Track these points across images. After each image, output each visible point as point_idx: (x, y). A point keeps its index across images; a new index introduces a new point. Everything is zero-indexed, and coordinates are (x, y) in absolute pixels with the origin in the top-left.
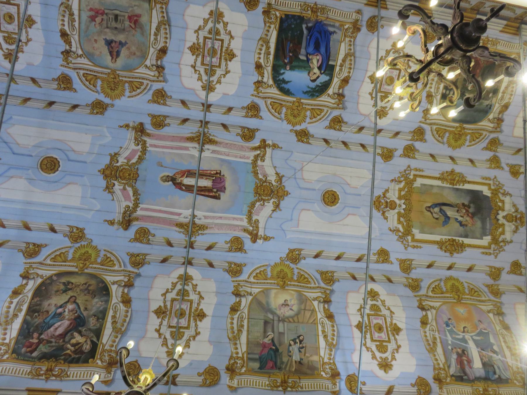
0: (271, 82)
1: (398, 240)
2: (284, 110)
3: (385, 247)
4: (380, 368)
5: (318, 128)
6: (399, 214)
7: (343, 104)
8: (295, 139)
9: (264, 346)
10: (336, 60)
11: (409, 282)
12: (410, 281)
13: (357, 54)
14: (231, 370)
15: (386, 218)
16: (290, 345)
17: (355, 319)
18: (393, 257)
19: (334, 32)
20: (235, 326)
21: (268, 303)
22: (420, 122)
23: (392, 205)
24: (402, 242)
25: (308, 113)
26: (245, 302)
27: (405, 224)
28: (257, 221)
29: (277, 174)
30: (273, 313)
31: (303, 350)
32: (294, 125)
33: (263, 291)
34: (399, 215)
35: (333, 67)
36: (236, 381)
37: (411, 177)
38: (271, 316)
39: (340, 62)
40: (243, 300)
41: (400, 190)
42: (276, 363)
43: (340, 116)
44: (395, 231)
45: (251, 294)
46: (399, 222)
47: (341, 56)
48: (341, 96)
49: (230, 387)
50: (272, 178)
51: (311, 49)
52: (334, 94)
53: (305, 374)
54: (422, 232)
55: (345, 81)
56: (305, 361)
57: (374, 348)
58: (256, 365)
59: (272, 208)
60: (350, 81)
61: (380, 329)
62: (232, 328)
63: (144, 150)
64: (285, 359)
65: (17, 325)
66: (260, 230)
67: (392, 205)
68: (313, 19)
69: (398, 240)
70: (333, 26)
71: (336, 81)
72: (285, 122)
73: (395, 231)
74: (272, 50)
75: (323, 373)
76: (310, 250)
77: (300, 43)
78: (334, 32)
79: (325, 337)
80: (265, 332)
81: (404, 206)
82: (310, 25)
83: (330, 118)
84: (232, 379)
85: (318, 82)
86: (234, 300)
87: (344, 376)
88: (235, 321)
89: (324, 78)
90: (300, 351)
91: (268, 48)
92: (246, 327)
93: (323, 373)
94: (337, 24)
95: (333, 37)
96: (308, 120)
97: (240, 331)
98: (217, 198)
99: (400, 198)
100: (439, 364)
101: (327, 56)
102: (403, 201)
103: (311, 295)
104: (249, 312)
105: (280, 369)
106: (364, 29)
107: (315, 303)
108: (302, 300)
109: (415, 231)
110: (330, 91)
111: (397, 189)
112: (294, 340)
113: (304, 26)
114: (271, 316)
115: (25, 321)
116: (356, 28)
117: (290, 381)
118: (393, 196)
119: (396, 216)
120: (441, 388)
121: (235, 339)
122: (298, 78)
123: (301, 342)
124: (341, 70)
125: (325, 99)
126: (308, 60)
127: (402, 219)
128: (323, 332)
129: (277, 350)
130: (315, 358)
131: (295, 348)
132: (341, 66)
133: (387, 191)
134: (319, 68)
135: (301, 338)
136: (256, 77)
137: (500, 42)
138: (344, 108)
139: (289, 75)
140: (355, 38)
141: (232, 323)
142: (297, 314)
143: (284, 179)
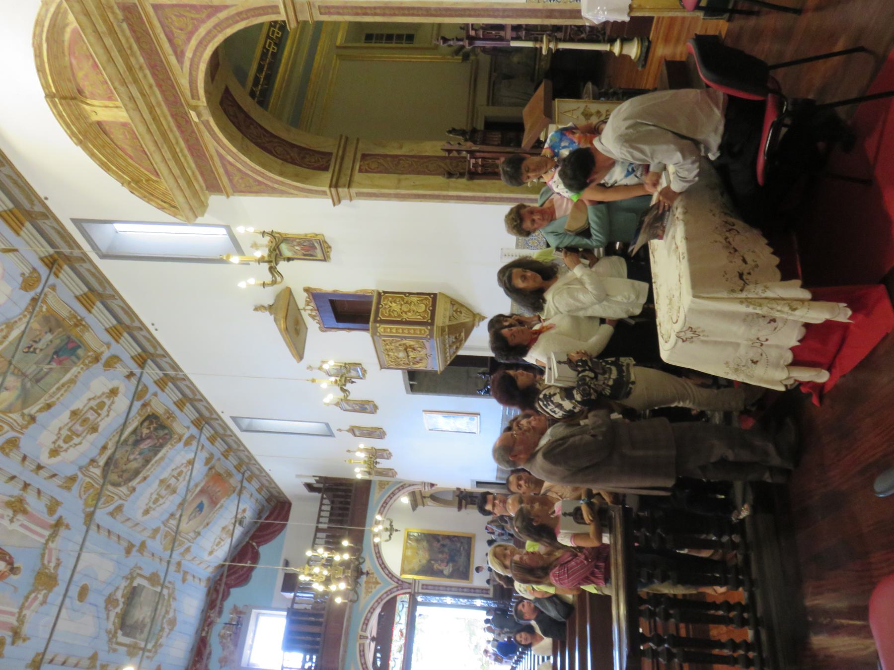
9: (60, 363)
14: (97, 359)
16: (41, 350)
20: (62, 392)
21: (17, 398)
26: (33, 410)
30: (23, 386)
31: (37, 339)
33: (10, 412)
36: (102, 349)
38: (29, 385)
42: (67, 344)
45: (23, 415)
49: (109, 348)
53: (56, 319)
56: (46, 329)
58: (80, 352)
62: (65, 391)
63: (21, 609)
64: (58, 341)
65: (160, 455)
75: (44, 309)
80: (47, 374)
84: (102, 353)
86: (40, 417)
88: (59, 395)
90: (40, 340)
92: (57, 386)
93: (44, 309)
97: (63, 386)
104: (40, 398)
105: (69, 337)
112: (34, 352)
114: (29, 385)
115: (156, 454)
117: (72, 323)
121: (72, 381)
123: (29, 348)
129: (56, 353)
135: (27, 350)
141: (62, 395)
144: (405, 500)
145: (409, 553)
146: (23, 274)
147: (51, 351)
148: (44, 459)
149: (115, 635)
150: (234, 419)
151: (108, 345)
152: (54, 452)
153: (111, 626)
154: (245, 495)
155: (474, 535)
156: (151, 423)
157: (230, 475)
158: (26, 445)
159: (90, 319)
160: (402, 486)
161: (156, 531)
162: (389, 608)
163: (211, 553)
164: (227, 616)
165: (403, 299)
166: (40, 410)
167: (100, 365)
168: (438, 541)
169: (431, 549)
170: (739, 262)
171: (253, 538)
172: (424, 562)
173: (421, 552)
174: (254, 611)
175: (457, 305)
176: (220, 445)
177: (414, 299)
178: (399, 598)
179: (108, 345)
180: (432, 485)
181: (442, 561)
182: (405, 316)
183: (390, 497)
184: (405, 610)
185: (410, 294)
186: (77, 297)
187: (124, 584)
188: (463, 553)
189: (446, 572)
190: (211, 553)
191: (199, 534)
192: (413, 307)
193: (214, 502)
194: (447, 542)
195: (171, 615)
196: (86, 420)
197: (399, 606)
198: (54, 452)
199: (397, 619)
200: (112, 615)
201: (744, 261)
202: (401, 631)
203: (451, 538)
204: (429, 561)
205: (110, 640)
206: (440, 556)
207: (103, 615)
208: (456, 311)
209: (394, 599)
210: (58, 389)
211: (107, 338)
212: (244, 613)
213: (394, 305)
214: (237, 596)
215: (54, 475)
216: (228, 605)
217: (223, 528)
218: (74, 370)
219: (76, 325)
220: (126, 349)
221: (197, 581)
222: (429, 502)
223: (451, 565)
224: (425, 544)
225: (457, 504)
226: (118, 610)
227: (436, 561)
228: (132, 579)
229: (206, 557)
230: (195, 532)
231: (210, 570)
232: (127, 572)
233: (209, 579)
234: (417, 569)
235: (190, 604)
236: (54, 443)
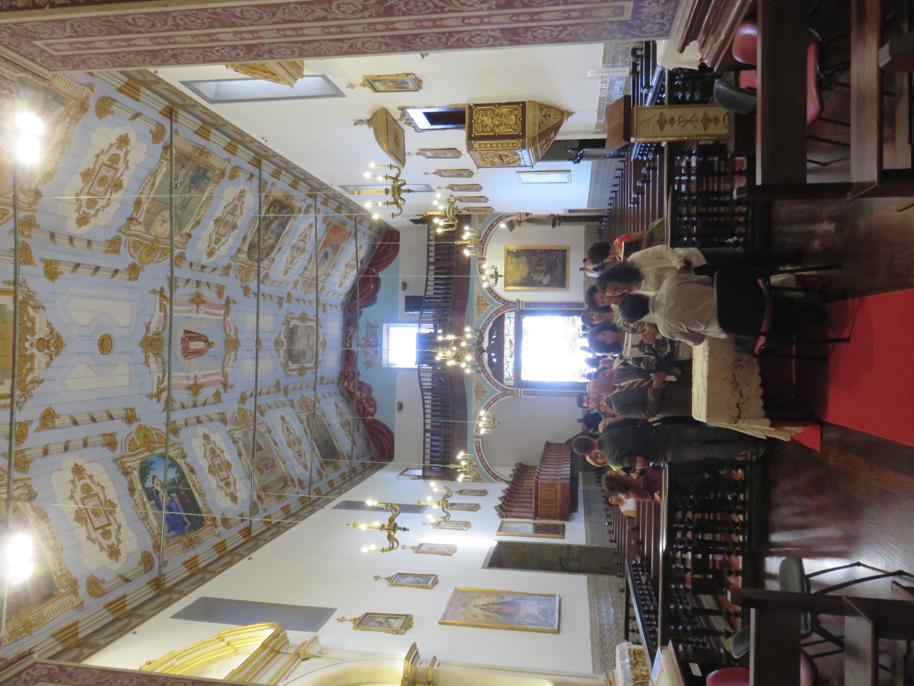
0: (178, 460)
1: (34, 293)
2: (156, 438)
3: (49, 282)
4: (129, 141)
5: (122, 430)
6: (33, 333)
7: (119, 465)
8: (136, 411)
9: (197, 188)
10: (152, 506)
11: (29, 231)
12: (26, 233)
13: (140, 522)
14: (223, 174)
15: (49, 324)
18: (40, 268)
19: (168, 532)
23: (42, 344)
24: (29, 291)
25: (138, 443)
26: (187, 229)
27: (25, 318)
28: (161, 310)
29: (149, 365)
32: (140, 426)
34: (32, 331)
35: (150, 499)
38: (179, 213)
39: (148, 506)
40: (188, 231)
41: (31, 369)
43: (113, 451)
44: (38, 307)
45: (181, 235)
46: (32, 320)
48: (126, 473)
49: (229, 162)
50: (152, 359)
52: (132, 472)
55: (132, 490)
56: (180, 167)
58: (209, 174)
59: (151, 325)
60: (128, 492)
61: (102, 180)
63: (223, 368)
64: (191, 173)
65: (287, 228)
66: (158, 301)
67: (42, 344)
68: (187, 534)
69: (34, 293)
70: (173, 537)
71: (138, 486)
72: (148, 427)
73: (38, 307)
74: (194, 491)
76: (122, 278)
78: (168, 532)
79: (153, 185)
81: (27, 345)
82: (186, 528)
83: (119, 445)
85: (150, 477)
86: (194, 233)
87: (162, 143)
89: (149, 484)
91: (197, 490)
94: (171, 541)
96: (134, 435)
98: (186, 332)
99: (32, 356)
100: (69, 123)
102: (28, 353)
103: (140, 228)
105: (198, 166)
106: (151, 550)
108: (148, 225)
109: (10, 308)
110: (136, 473)
111: (36, 371)
113: (189, 524)
114: (179, 213)
115: (284, 229)
116: (157, 547)
118: (41, 358)
119: (37, 330)
120: (87, 98)
121: (210, 198)
122: (161, 475)
124: (142, 499)
125: (134, 463)
127: (30, 325)
129: (192, 181)
132: (144, 503)
133: (48, 365)
134: (157, 492)
136: (188, 459)
137: (9, 640)
138: (115, 461)
139: (172, 474)
140: (153, 537)
142: (161, 210)
143: (143, 361)
144: (503, 226)
145: (510, 268)
146: (151, 131)
147: (188, 181)
148: (205, 260)
149: (287, 366)
150: (341, 187)
151: (229, 160)
152: (211, 253)
153: (283, 360)
154: (360, 235)
155: (569, 248)
156: (275, 207)
157: (344, 224)
158: (190, 257)
159: (209, 146)
160: (501, 218)
161: (297, 282)
162: (499, 324)
163: (340, 285)
164: (362, 332)
165: (493, 111)
166: (193, 228)
167: (226, 178)
168: (536, 255)
169: (530, 263)
170: (738, 395)
171: (370, 265)
172: (524, 274)
173: (520, 266)
174: (385, 325)
175: (546, 109)
176: (333, 204)
177: (504, 110)
178: (506, 315)
179: (229, 160)
180: (527, 214)
181: (540, 273)
182: (497, 130)
183: (490, 229)
184: (513, 324)
185: (500, 104)
186: (196, 132)
187: (283, 328)
188: (559, 264)
189: (544, 282)
190: (340, 285)
191: (329, 275)
192: (504, 120)
193: (336, 248)
194: (545, 255)
195: (321, 339)
196: (226, 223)
197: (507, 322)
198: (211, 253)
199: (506, 331)
200: (282, 352)
201: (741, 395)
202: (510, 341)
203: (548, 252)
204: (529, 273)
205: (285, 370)
206: (539, 268)
207: (275, 354)
208: (545, 116)
209: (503, 316)
210: (201, 208)
211: (226, 155)
212: (377, 327)
213: (485, 118)
214: (368, 314)
215: (215, 269)
216: (362, 322)
217: (347, 265)
218: (209, 189)
219: (201, 155)
220: (243, 158)
221: (334, 308)
222: (526, 223)
223: (549, 275)
224: (524, 259)
225: (551, 222)
226: (285, 348)
227: (535, 273)
228: (288, 323)
229: (337, 289)
230: (325, 274)
231: (342, 297)
232: (283, 319)
233: (342, 304)
234: (518, 281)
235: (333, 326)
236: (208, 247)
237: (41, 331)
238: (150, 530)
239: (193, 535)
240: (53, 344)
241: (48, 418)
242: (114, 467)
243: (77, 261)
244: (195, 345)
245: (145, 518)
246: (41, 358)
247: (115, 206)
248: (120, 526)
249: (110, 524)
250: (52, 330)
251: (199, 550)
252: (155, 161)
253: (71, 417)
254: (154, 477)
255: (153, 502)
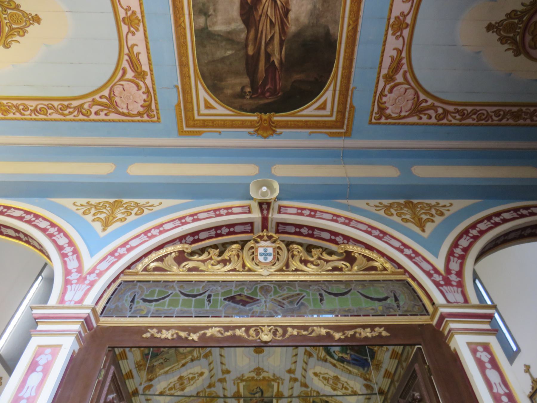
3: (231, 373)
10: (347, 365)
15: (250, 372)
17: (184, 374)
22: (312, 389)
23: (258, 374)
34: (253, 378)
37: (278, 381)
44: (243, 376)
46: (248, 377)
47: (349, 368)
48: (326, 361)
51: (353, 357)
54: (244, 386)
55: (334, 365)
57: (170, 387)
67: (258, 374)
71: (335, 362)
73: (243, 376)
77: (357, 353)
79: (172, 368)
85: (333, 353)
89: (336, 357)
94: (369, 372)
95: (361, 369)
101: (348, 362)
106: (365, 382)
107: (190, 357)
109: (244, 383)
110: (328, 357)
116: (366, 379)
118: (264, 375)
126: (347, 354)
128: (174, 367)
130: (157, 370)
131: (161, 361)
133: (267, 372)
134: (342, 357)
140: (361, 377)
142: (181, 354)
159: (133, 367)
219: (141, 366)
237: (253, 375)
238: (357, 375)
239: (375, 362)
240: (258, 371)
241: (290, 371)
242: (320, 362)
243: (219, 356)
244: (265, 206)
245: (350, 372)
246: (264, 375)
247: (189, 371)
248: (346, 382)
249: (343, 385)
250: (252, 371)
251: (385, 366)
252: (160, 378)
253: (292, 364)
254: (334, 352)
255: (345, 363)
